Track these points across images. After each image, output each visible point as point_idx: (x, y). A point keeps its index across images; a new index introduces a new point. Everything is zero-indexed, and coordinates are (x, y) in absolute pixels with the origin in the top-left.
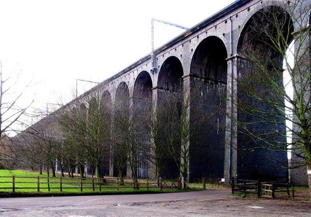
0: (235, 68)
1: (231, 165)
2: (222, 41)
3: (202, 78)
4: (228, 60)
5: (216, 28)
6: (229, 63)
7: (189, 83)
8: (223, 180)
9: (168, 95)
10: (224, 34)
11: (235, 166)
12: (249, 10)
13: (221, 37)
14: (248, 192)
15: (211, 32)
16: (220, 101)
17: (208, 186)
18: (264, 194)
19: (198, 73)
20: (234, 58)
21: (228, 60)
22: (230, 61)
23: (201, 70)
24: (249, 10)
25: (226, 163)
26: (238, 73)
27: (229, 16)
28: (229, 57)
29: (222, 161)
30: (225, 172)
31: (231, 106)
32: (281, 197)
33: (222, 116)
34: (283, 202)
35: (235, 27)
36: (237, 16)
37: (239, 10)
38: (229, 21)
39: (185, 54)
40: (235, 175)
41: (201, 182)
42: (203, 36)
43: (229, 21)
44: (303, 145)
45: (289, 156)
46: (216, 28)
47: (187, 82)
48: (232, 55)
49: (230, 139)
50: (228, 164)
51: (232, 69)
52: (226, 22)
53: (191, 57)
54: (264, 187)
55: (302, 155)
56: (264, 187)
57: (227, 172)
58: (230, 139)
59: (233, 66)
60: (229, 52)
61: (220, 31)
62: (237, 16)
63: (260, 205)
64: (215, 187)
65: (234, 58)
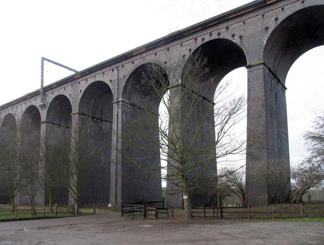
0: (120, 110)
1: (116, 192)
2: (108, 86)
3: (89, 116)
4: (115, 103)
5: (104, 74)
6: (115, 106)
7: (45, 129)
8: (110, 205)
9: (58, 131)
10: (111, 81)
11: (119, 193)
12: (133, 63)
13: (108, 82)
14: (136, 215)
15: (99, 77)
16: (105, 136)
17: (98, 211)
18: (149, 215)
19: (86, 112)
20: (119, 102)
21: (115, 103)
22: (116, 104)
23: (88, 109)
24: (133, 63)
25: (111, 191)
26: (122, 115)
27: (116, 66)
28: (115, 100)
29: (108, 189)
30: (111, 198)
31: (116, 140)
32: (162, 218)
33: (108, 149)
34: (164, 221)
35: (121, 76)
36: (123, 67)
37: (124, 62)
38: (115, 70)
39: (74, 95)
40: (120, 200)
41: (92, 207)
42: (91, 80)
43: (115, 70)
44: (181, 177)
45: (164, 184)
46: (104, 74)
47: (75, 120)
48: (117, 99)
49: (115, 172)
50: (113, 192)
51: (117, 112)
52: (113, 70)
53: (80, 98)
54: (149, 210)
55: (180, 184)
56: (149, 210)
57: (112, 198)
58: (115, 172)
59: (118, 108)
60: (115, 97)
61: (107, 77)
62: (123, 67)
63: (149, 224)
64: (104, 211)
65: (119, 102)
